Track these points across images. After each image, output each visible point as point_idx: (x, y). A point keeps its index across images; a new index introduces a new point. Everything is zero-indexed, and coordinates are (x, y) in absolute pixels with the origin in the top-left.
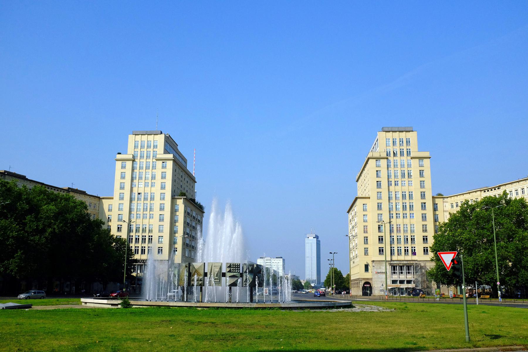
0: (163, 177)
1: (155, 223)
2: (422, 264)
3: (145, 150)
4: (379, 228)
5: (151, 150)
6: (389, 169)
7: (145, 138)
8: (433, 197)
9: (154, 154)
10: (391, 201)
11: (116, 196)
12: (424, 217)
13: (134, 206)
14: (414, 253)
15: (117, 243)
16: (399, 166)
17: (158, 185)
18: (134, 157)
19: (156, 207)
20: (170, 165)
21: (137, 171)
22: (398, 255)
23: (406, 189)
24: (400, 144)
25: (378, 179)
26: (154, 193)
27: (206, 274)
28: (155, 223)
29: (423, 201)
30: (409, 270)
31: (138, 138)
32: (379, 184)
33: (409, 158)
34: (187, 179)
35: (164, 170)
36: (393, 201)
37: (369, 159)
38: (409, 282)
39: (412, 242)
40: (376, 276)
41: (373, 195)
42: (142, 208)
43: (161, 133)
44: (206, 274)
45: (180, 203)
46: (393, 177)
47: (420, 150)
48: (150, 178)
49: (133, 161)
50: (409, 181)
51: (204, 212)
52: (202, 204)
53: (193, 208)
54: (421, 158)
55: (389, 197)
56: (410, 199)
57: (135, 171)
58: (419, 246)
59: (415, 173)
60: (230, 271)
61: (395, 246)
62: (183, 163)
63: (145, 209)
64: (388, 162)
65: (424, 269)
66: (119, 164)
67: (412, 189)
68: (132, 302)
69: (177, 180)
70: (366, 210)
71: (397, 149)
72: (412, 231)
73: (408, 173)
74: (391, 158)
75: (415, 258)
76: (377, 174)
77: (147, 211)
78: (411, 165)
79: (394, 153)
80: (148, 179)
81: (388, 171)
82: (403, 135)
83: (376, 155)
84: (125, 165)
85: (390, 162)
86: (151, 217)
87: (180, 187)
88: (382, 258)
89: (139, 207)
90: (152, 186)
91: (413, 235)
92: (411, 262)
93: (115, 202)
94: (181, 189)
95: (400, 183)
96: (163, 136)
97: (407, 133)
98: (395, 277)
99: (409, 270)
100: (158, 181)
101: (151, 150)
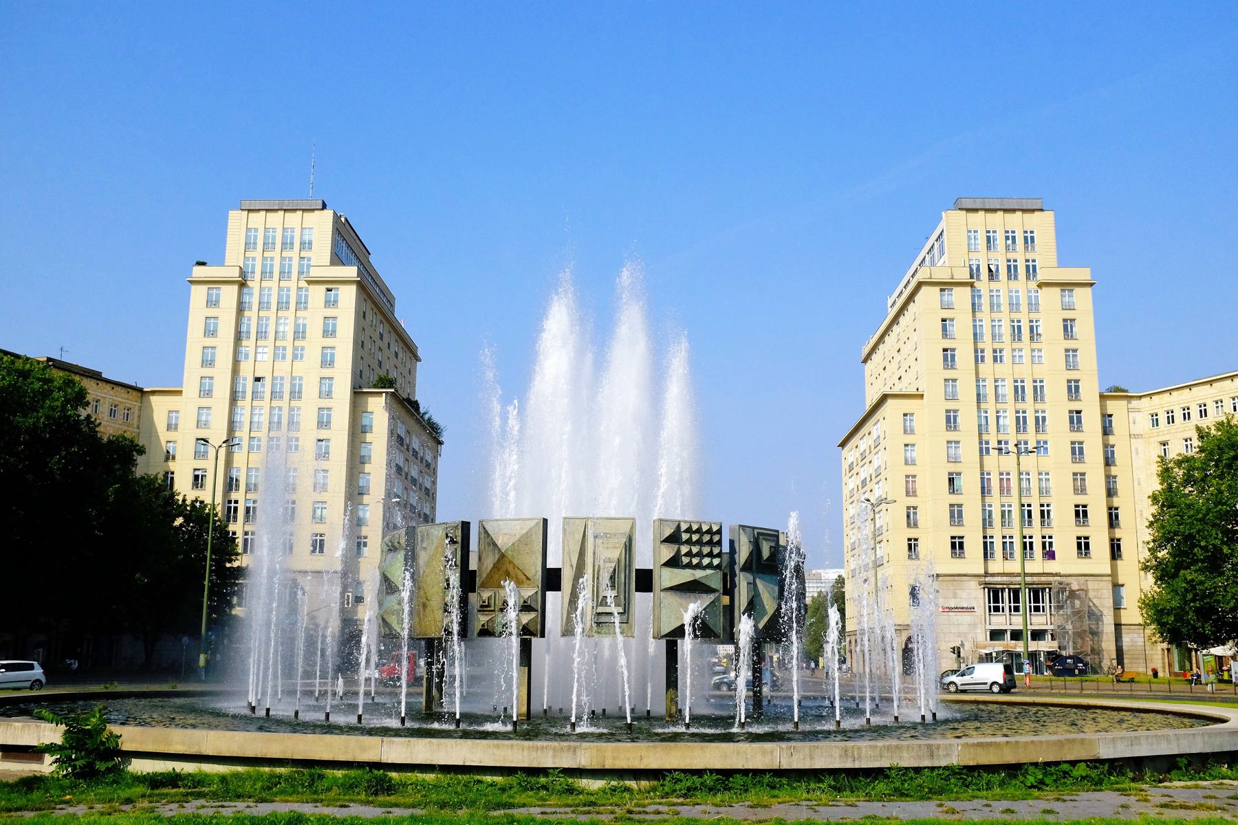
0: (329, 332)
2: (1075, 587)
3: (276, 254)
4: (951, 481)
5: (294, 254)
6: (978, 315)
7: (276, 219)
8: (1102, 397)
9: (301, 266)
10: (983, 406)
11: (190, 386)
12: (1077, 452)
13: (243, 416)
14: (1050, 555)
15: (188, 520)
16: (1005, 307)
18: (243, 273)
19: (308, 418)
20: (348, 296)
21: (251, 314)
22: (1005, 558)
23: (1025, 372)
24: (1007, 247)
25: (947, 344)
26: (301, 378)
27: (552, 579)
29: (1075, 406)
30: (1036, 600)
31: (257, 219)
32: (949, 356)
33: (1033, 285)
34: (394, 348)
35: (330, 312)
36: (990, 405)
37: (920, 285)
38: (1038, 635)
39: (1042, 523)
40: (944, 618)
41: (933, 388)
42: (264, 419)
43: (324, 207)
44: (552, 579)
45: (378, 407)
46: (987, 337)
47: (1062, 263)
48: (290, 336)
49: (242, 285)
50: (1033, 350)
51: (441, 443)
52: (435, 419)
53: (415, 428)
54: (1067, 286)
55: (978, 395)
56: (1035, 399)
57: (247, 313)
58: (1064, 534)
59: (1050, 326)
60: (674, 563)
61: (997, 533)
63: (274, 425)
64: (973, 297)
65: (1079, 598)
66: (198, 294)
67: (1040, 372)
68: (130, 737)
69: (368, 345)
70: (912, 432)
71: (999, 258)
72: (1043, 492)
73: (1031, 328)
74: (983, 285)
75: (1051, 566)
76: (944, 329)
78: (1037, 304)
79: (990, 270)
80: (284, 338)
81: (974, 321)
82: (1016, 221)
83: (942, 275)
84: (218, 295)
85: (980, 297)
87: (375, 366)
88: (957, 566)
89: (256, 419)
90: (295, 357)
91: (1045, 501)
92: (1043, 579)
93: (187, 405)
95: (1007, 354)
96: (328, 215)
97: (1027, 216)
98: (999, 621)
99: (1036, 600)
100: (314, 343)
101: (294, 254)
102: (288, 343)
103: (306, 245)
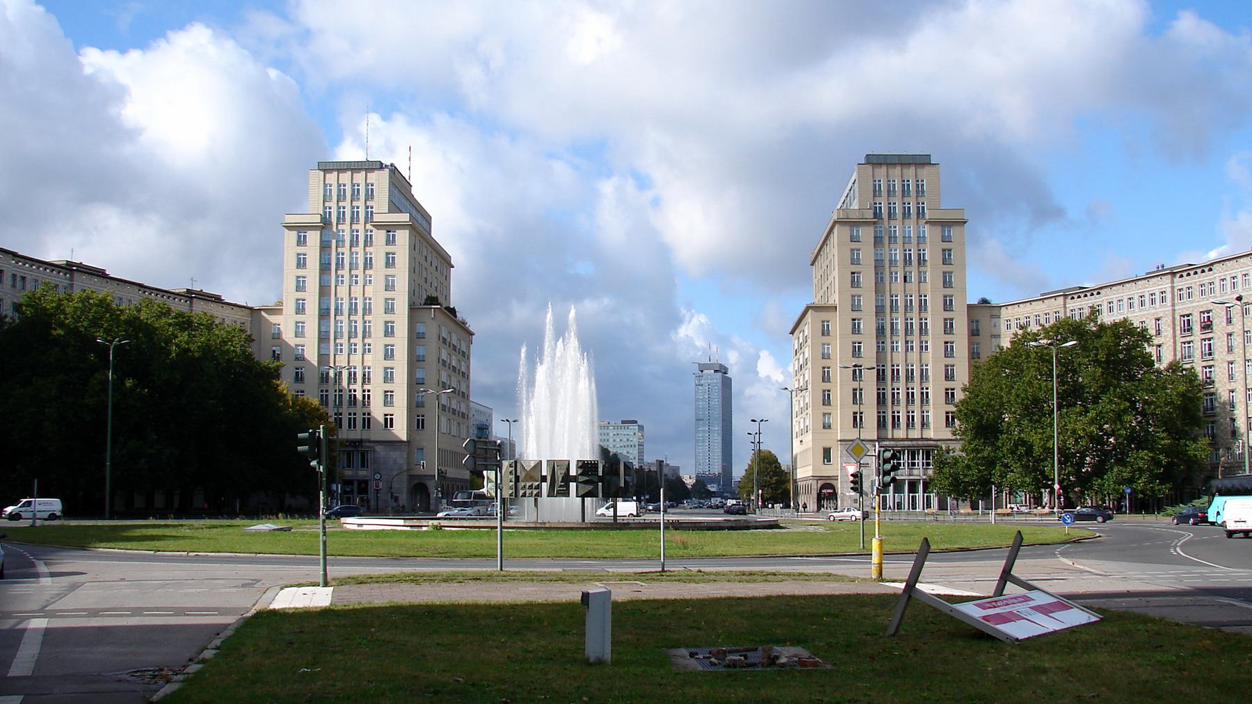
1: (375, 362)
11: (289, 307)
19: (377, 329)
20: (403, 237)
27: (544, 479)
28: (375, 362)
44: (544, 479)
51: (472, 334)
62: (425, 225)
86: (366, 350)
87: (422, 282)
103: (370, 195)
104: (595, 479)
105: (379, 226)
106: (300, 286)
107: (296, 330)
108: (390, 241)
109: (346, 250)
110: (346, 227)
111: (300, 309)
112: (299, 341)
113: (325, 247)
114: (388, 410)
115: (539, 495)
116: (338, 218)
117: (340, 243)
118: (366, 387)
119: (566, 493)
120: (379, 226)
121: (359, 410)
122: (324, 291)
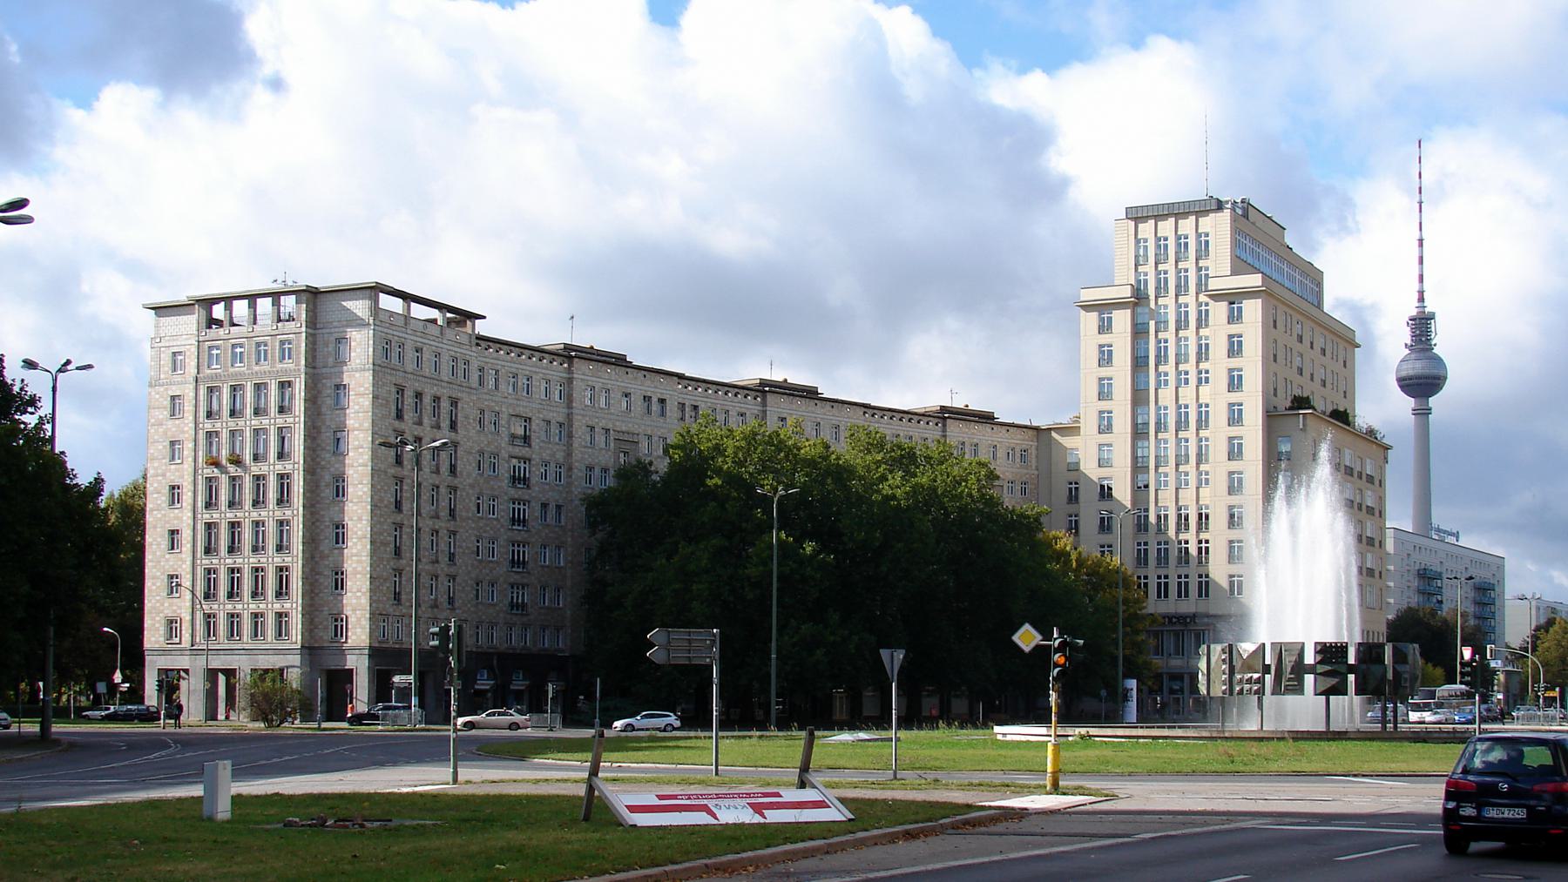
11: (1089, 425)
17: (1219, 379)
19: (1218, 450)
20: (1253, 310)
27: (1266, 669)
28: (1215, 500)
44: (1266, 669)
77: (1187, 462)
87: (1292, 374)
94: (1298, 379)
96: (1227, 213)
100: (1218, 363)
102: (1190, 367)
103: (1203, 250)
104: (1343, 669)
105: (1217, 297)
106: (1104, 393)
107: (1100, 456)
108: (1234, 317)
109: (1170, 335)
110: (1169, 301)
111: (1105, 427)
112: (1104, 472)
113: (1139, 332)
114: (1234, 569)
115: (1260, 693)
116: (1157, 288)
117: (1161, 325)
118: (1203, 536)
119: (1298, 689)
120: (1217, 297)
121: (1193, 571)
122: (1139, 397)
